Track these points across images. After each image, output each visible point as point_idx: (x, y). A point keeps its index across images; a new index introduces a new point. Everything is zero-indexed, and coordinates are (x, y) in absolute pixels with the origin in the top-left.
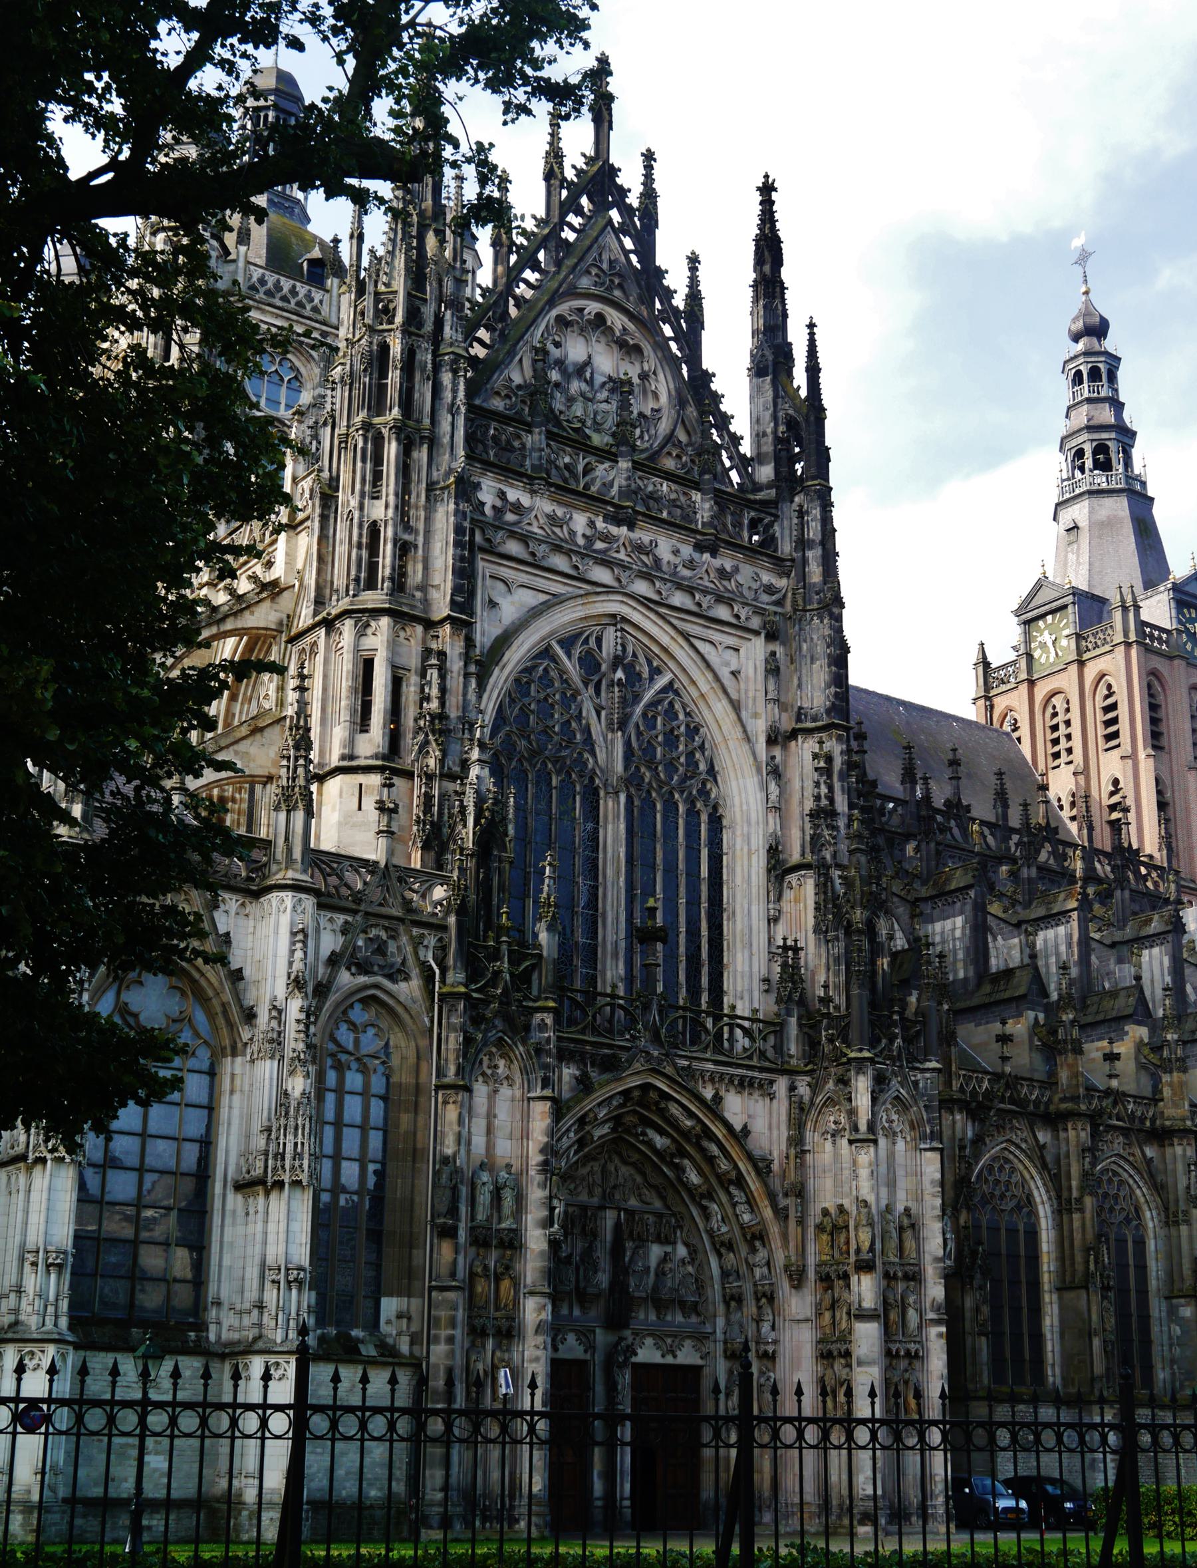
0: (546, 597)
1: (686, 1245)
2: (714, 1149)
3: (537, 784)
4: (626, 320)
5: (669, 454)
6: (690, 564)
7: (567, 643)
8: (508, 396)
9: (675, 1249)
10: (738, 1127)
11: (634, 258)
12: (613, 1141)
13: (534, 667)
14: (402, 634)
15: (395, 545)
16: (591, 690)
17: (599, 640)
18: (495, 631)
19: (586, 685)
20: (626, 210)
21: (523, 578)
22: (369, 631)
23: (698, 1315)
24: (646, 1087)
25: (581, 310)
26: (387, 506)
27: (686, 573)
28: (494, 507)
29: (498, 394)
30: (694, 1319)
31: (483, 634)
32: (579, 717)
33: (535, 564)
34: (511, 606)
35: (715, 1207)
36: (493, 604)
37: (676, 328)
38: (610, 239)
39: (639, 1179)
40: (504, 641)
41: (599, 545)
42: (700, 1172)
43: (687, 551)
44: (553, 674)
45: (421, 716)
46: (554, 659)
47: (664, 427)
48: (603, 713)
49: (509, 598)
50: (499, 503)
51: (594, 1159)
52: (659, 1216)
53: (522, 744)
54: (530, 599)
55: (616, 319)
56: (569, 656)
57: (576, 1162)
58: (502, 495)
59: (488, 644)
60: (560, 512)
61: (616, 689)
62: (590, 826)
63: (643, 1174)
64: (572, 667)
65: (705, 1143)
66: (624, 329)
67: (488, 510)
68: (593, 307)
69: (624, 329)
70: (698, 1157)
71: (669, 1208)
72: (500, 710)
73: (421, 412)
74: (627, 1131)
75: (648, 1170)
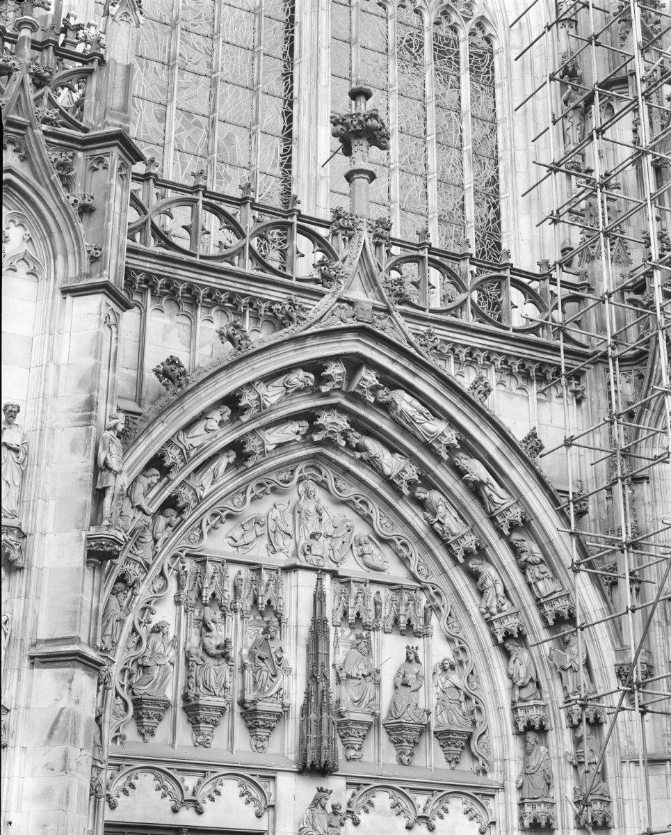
1: (450, 640)
2: (477, 470)
9: (428, 649)
10: (519, 434)
12: (316, 461)
23: (474, 758)
24: (354, 363)
30: (466, 764)
35: (488, 571)
39: (361, 530)
42: (463, 515)
51: (274, 490)
52: (397, 588)
57: (241, 490)
63: (367, 519)
65: (466, 462)
70: (458, 489)
71: (419, 581)
74: (329, 442)
75: (375, 516)
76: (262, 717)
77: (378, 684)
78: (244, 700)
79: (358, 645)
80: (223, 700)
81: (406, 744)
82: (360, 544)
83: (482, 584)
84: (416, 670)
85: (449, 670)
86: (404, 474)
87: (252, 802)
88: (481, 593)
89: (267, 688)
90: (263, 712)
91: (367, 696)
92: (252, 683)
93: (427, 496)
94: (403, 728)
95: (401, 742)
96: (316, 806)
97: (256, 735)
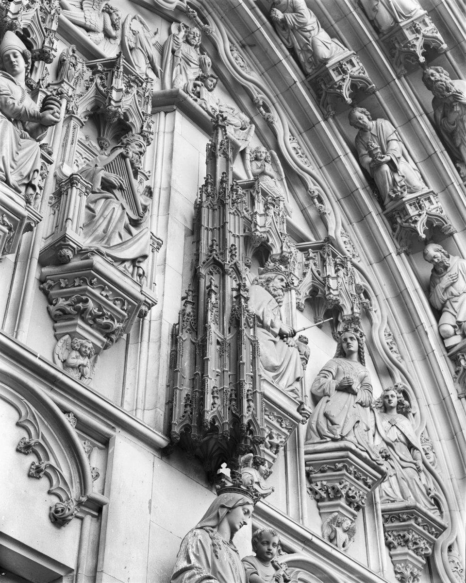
76: (97, 292)
77: (305, 359)
78: (64, 238)
79: (268, 281)
80: (23, 203)
81: (342, 502)
82: (257, 159)
83: (446, 289)
84: (363, 374)
85: (395, 410)
86: (349, 66)
87: (44, 481)
88: (438, 313)
89: (116, 240)
90: (106, 283)
91: (291, 368)
92: (83, 220)
93: (371, 124)
94: (346, 463)
95: (337, 494)
96: (218, 526)
97: (73, 335)
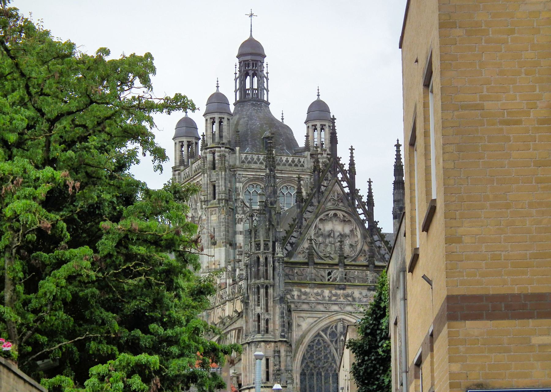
0: (315, 319)
3: (317, 375)
4: (344, 213)
5: (361, 255)
6: (366, 296)
7: (325, 330)
8: (303, 253)
11: (347, 190)
13: (314, 340)
14: (268, 346)
15: (264, 320)
16: (334, 343)
17: (336, 327)
18: (301, 333)
19: (332, 341)
20: (344, 172)
21: (309, 315)
22: (259, 346)
25: (328, 215)
26: (261, 309)
27: (365, 300)
28: (298, 295)
29: (300, 253)
31: (296, 336)
32: (330, 352)
33: (312, 311)
34: (305, 325)
36: (299, 325)
37: (364, 209)
38: (337, 187)
40: (303, 337)
41: (334, 298)
43: (365, 292)
44: (321, 341)
45: (273, 371)
46: (321, 336)
47: (359, 247)
48: (338, 350)
49: (305, 322)
50: (299, 294)
53: (311, 365)
54: (311, 320)
55: (340, 214)
56: (326, 334)
58: (300, 291)
59: (298, 338)
60: (319, 291)
61: (341, 343)
62: (335, 385)
64: (327, 338)
66: (344, 216)
67: (296, 297)
68: (332, 212)
69: (344, 216)
72: (304, 356)
73: (270, 277)
